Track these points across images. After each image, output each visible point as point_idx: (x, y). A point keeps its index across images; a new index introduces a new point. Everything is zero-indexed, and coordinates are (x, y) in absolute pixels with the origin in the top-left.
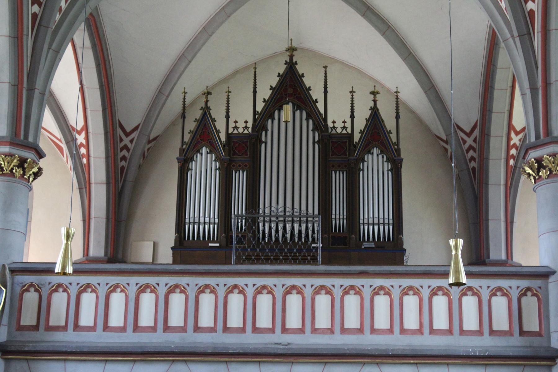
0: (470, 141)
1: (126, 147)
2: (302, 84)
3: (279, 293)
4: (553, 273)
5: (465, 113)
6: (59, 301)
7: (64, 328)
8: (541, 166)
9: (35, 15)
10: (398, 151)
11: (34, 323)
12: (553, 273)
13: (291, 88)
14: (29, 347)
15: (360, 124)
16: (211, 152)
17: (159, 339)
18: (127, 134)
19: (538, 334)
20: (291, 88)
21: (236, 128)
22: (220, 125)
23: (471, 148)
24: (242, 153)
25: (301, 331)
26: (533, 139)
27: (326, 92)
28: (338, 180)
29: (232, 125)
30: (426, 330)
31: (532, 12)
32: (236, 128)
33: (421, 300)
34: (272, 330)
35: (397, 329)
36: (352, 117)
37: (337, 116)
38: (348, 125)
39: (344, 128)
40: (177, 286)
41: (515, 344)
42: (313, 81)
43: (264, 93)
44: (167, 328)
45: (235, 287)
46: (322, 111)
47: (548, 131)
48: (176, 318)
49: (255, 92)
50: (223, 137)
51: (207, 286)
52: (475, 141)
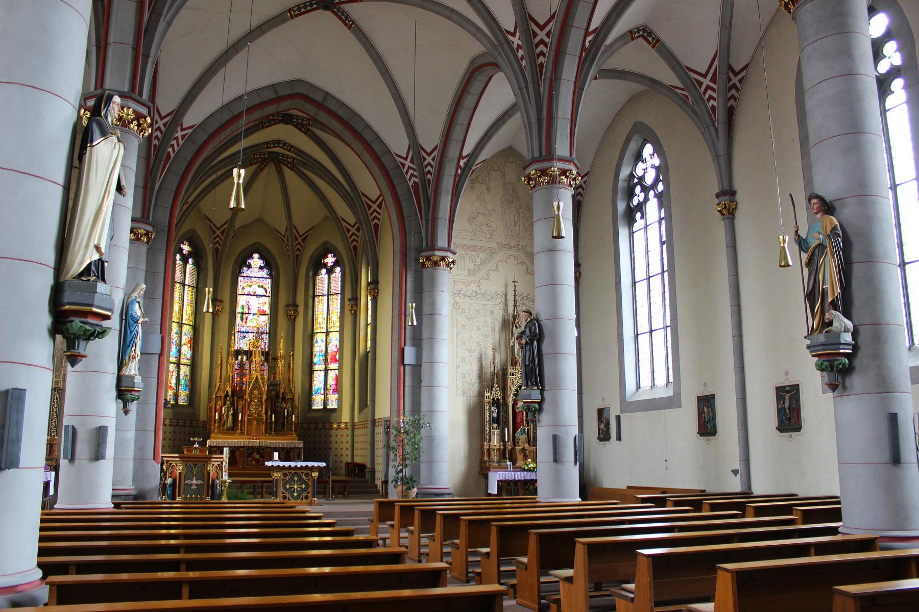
23: (429, 164)
52: (433, 160)
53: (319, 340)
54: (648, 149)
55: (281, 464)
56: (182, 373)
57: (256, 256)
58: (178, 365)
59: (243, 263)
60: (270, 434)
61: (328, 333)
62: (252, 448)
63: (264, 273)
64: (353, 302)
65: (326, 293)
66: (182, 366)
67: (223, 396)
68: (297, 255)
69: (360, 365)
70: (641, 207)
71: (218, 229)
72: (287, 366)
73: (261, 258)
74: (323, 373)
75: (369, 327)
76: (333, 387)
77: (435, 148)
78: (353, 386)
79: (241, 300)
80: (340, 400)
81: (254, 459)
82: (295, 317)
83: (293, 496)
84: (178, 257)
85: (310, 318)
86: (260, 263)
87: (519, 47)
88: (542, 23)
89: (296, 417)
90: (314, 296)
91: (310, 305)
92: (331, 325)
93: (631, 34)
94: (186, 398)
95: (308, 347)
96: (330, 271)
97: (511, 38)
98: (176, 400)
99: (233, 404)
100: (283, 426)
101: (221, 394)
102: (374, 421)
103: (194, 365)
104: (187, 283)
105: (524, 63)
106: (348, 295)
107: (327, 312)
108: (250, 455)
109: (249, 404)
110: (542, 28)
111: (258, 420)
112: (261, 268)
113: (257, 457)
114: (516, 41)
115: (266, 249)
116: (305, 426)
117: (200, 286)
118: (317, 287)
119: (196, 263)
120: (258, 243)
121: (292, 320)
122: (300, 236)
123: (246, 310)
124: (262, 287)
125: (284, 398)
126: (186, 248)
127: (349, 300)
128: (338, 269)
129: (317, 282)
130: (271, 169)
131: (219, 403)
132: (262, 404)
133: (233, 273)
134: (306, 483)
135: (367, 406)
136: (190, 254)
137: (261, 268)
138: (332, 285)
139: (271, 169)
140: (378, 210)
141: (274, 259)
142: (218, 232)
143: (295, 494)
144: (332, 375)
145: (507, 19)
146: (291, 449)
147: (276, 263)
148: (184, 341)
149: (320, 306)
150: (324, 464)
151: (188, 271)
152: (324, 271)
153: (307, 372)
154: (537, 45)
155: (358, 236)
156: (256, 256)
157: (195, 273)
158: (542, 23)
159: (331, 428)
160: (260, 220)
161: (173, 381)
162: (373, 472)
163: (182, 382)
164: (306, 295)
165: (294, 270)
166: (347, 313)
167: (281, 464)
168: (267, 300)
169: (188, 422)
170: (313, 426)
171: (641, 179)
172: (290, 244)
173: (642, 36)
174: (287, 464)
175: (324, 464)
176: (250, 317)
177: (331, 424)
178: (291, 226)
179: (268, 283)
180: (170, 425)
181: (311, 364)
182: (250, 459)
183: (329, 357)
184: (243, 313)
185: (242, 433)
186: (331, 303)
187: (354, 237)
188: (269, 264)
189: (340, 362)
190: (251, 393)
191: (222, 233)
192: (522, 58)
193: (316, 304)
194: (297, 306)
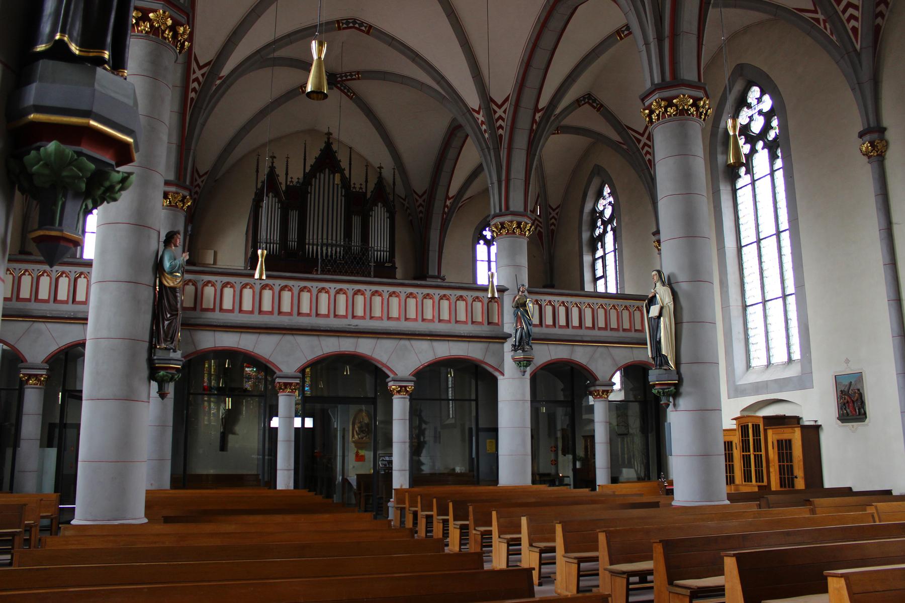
0: (420, 201)
1: (198, 185)
2: (336, 158)
3: (350, 293)
4: (507, 289)
5: (420, 184)
6: (209, 291)
7: (213, 310)
8: (503, 227)
9: (192, 99)
10: (394, 206)
11: (192, 305)
12: (507, 289)
13: (328, 160)
14: (192, 321)
15: (371, 186)
16: (275, 197)
17: (275, 320)
18: (200, 177)
19: (497, 324)
20: (328, 160)
21: (291, 182)
22: (282, 179)
24: (294, 199)
25: (363, 318)
26: (498, 211)
27: (350, 164)
28: (356, 221)
29: (289, 180)
30: (436, 320)
31: (501, 136)
32: (291, 182)
33: (434, 302)
34: (346, 317)
35: (420, 318)
36: (366, 181)
37: (357, 179)
38: (363, 186)
39: (361, 188)
40: (286, 286)
41: (485, 330)
42: (343, 158)
43: (311, 161)
44: (280, 313)
45: (323, 288)
46: (348, 176)
47: (507, 208)
48: (267, 306)
49: (305, 159)
50: (284, 188)
51: (305, 287)
54: (607, 190)
70: (601, 237)
77: (425, 193)
87: (483, 123)
88: (499, 103)
93: (578, 103)
97: (476, 115)
105: (487, 136)
110: (500, 107)
114: (481, 117)
145: (473, 100)
154: (497, 120)
158: (499, 103)
171: (602, 213)
173: (590, 104)
192: (485, 131)
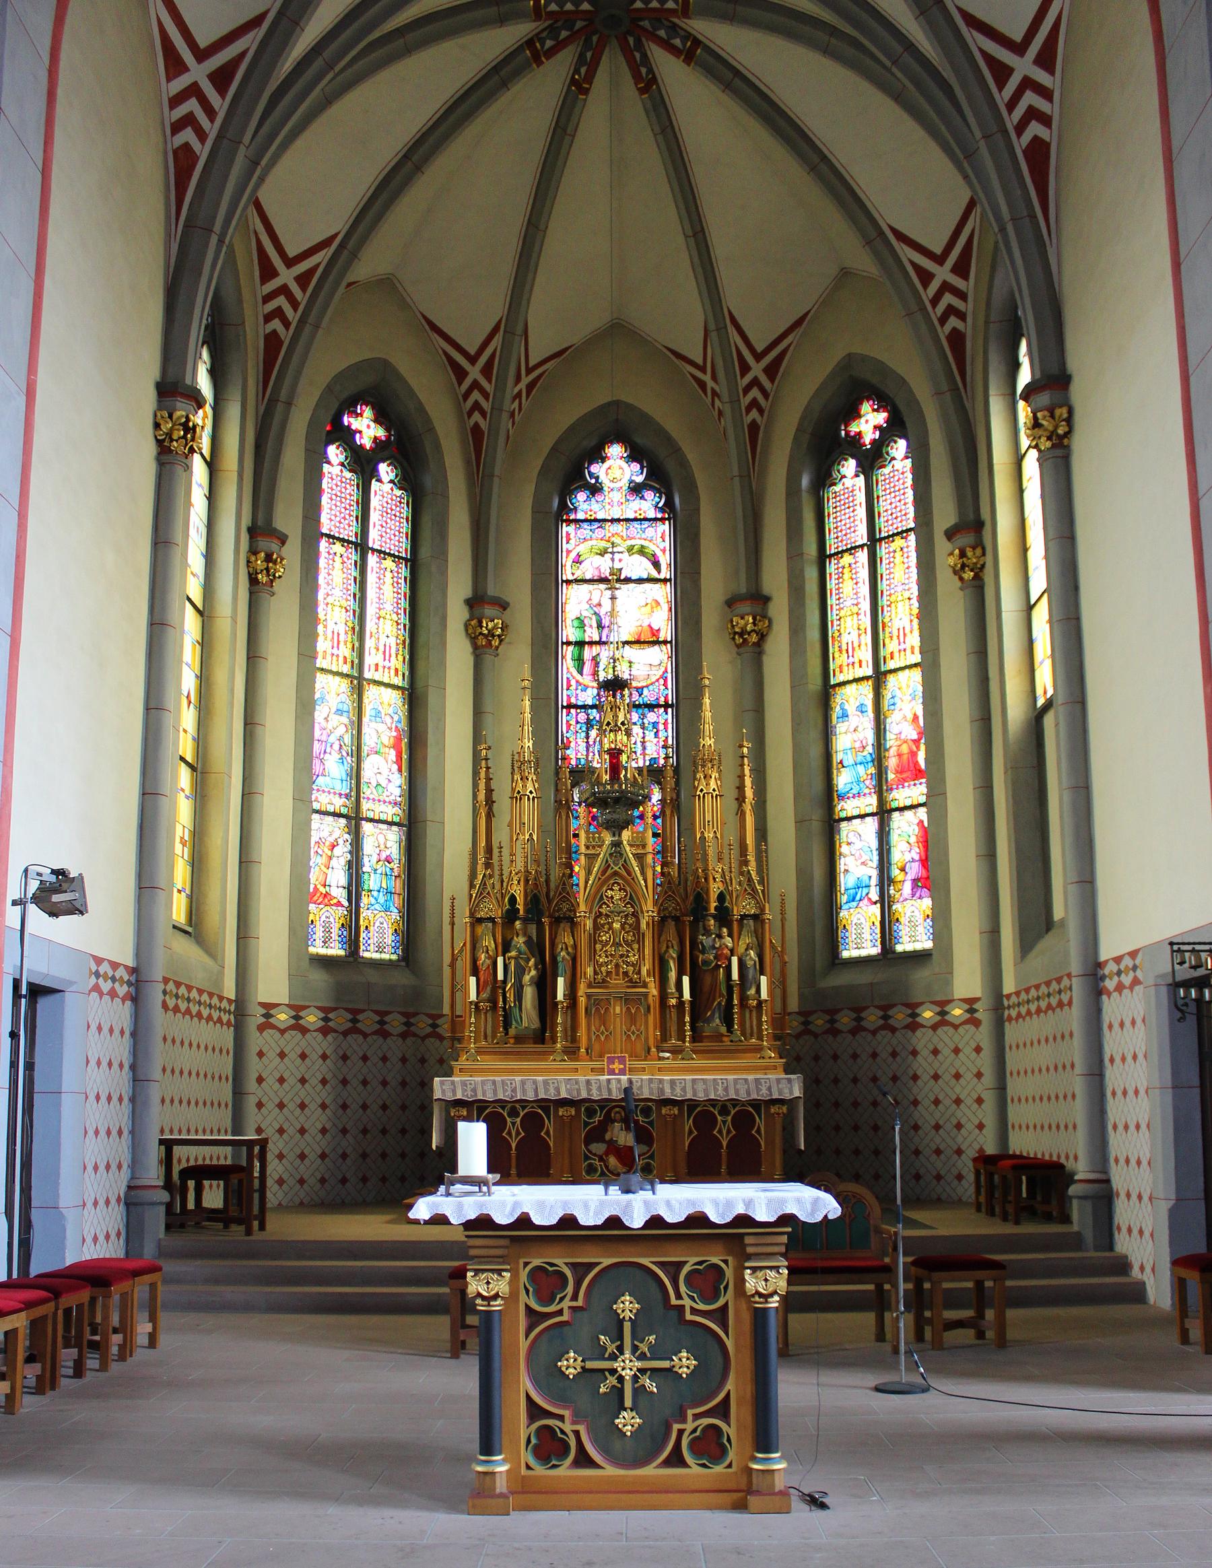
53: (851, 708)
55: (509, 1202)
56: (369, 847)
57: (615, 451)
58: (355, 820)
59: (572, 475)
60: (675, 1051)
61: (879, 678)
62: (603, 1103)
63: (648, 505)
64: (966, 539)
65: (861, 535)
66: (367, 827)
67: (497, 913)
68: (754, 427)
69: (1013, 768)
71: (473, 360)
72: (732, 794)
73: (634, 455)
74: (872, 824)
75: (1041, 615)
76: (914, 870)
78: (989, 855)
79: (576, 602)
80: (941, 919)
81: (613, 1148)
82: (762, 637)
83: (608, 1435)
84: (335, 453)
85: (814, 634)
86: (634, 472)
89: (780, 984)
90: (823, 557)
91: (812, 587)
92: (891, 646)
94: (389, 938)
95: (815, 735)
96: (871, 460)
98: (352, 940)
99: (537, 947)
100: (728, 1021)
101: (491, 908)
102: (1094, 973)
103: (414, 824)
104: (375, 538)
106: (945, 515)
107: (873, 598)
108: (596, 1134)
109: (593, 940)
111: (627, 1000)
112: (636, 490)
113: (625, 1138)
115: (647, 420)
116: (819, 1022)
117: (425, 552)
118: (830, 524)
119: (409, 482)
120: (617, 403)
121: (750, 647)
122: (758, 357)
123: (592, 634)
124: (642, 551)
125: (723, 916)
126: (366, 428)
127: (950, 534)
128: (900, 448)
129: (829, 508)
130: (612, 69)
131: (488, 942)
132: (640, 938)
133: (539, 510)
134: (706, 1344)
135: (1049, 924)
136: (381, 449)
137: (636, 490)
138: (882, 506)
139: (612, 69)
140: (1042, 77)
141: (676, 450)
142: (474, 373)
143: (628, 1421)
144: (905, 828)
146: (756, 1104)
147: (684, 463)
148: (370, 738)
149: (847, 587)
150: (811, 1203)
151: (375, 502)
152: (849, 467)
153: (816, 826)
155: (963, 296)
156: (615, 451)
157: (406, 512)
159: (914, 1026)
160: (618, 330)
161: (338, 878)
162: (1104, 1198)
163: (372, 882)
164: (794, 555)
165: (745, 477)
166: (947, 583)
167: (509, 1202)
168: (663, 593)
169: (395, 1023)
170: (845, 1020)
172: (722, 389)
174: (544, 1202)
175: (811, 1203)
176: (605, 654)
177: (913, 1008)
178: (720, 320)
179: (659, 539)
180: (325, 1031)
181: (829, 795)
182: (598, 1148)
183: (892, 762)
184: (581, 644)
185: (572, 1052)
186: (882, 569)
187: (948, 299)
188: (659, 474)
189: (934, 775)
190: (597, 899)
191: (487, 371)
193: (831, 585)
194: (766, 600)
